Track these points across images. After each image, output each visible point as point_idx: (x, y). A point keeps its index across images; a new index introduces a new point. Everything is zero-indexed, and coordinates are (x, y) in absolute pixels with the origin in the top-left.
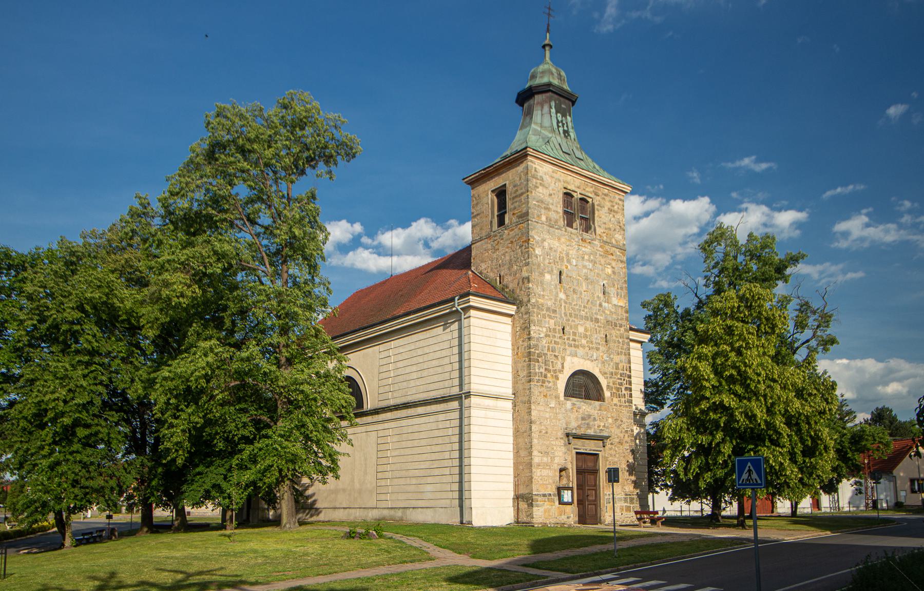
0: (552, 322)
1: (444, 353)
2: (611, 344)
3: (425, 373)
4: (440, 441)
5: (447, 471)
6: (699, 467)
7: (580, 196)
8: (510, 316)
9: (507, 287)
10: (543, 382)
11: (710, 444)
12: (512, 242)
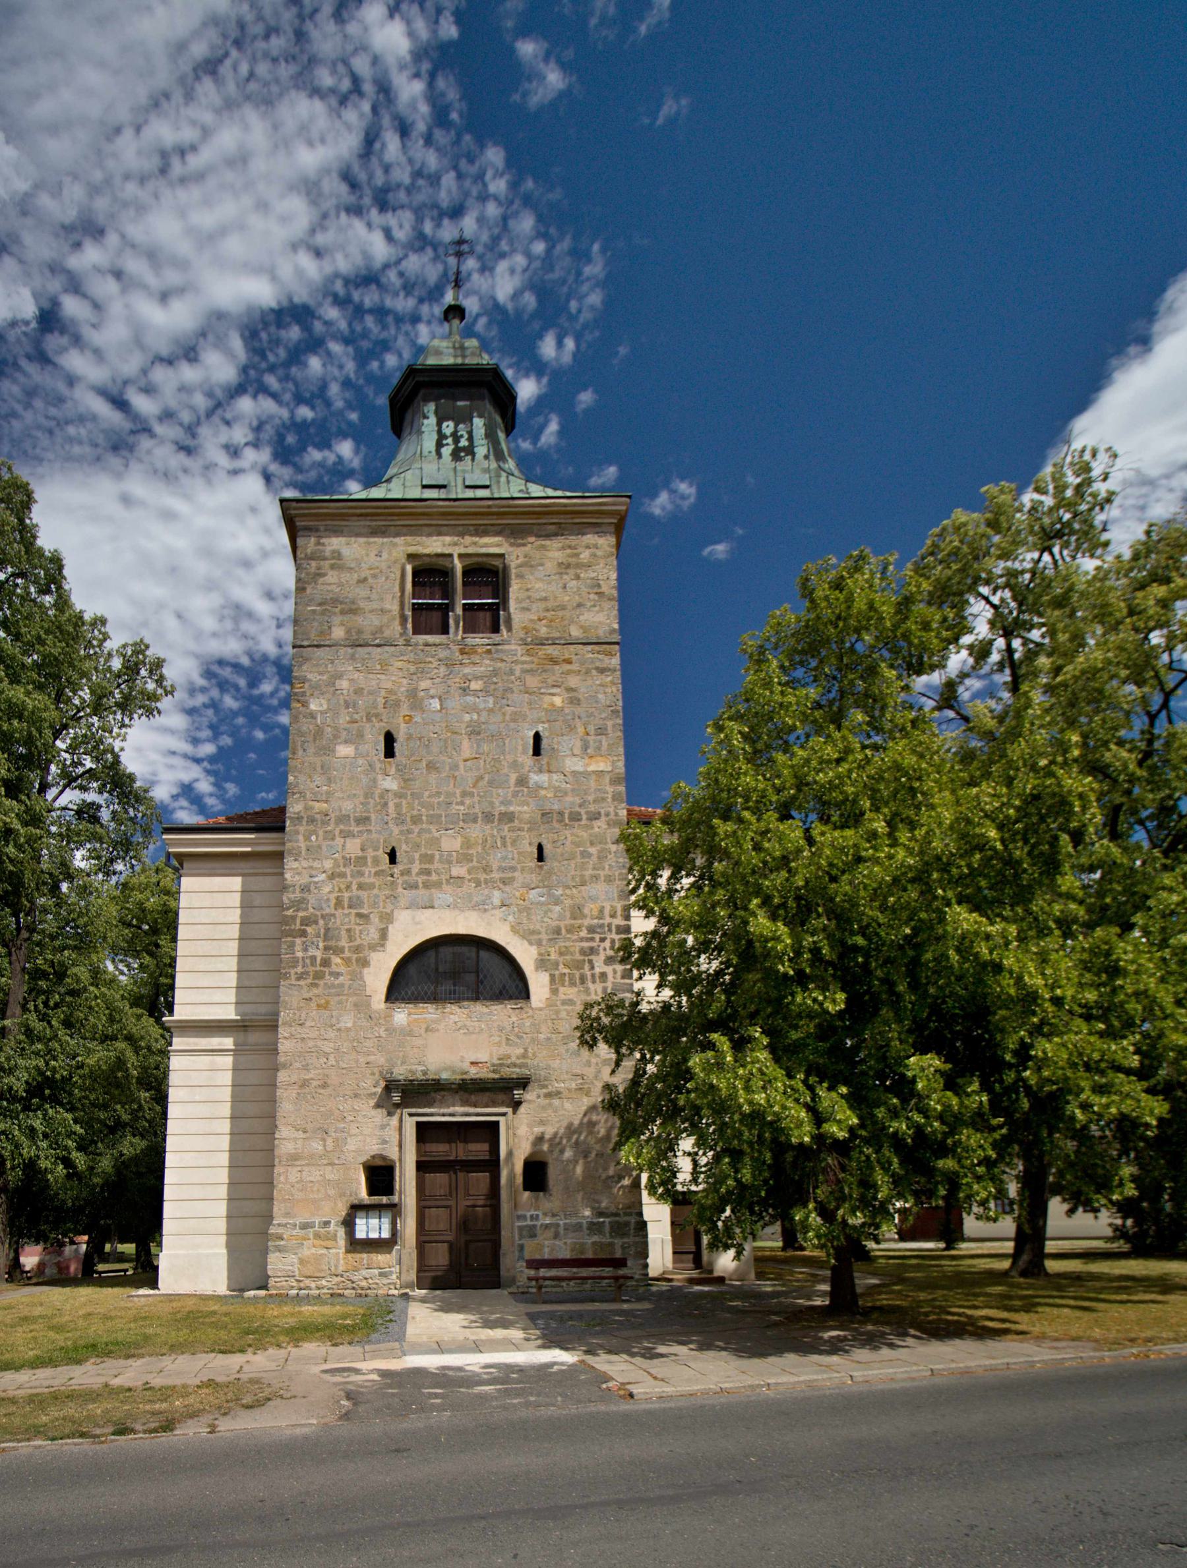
0: (353, 847)
10: (319, 976)
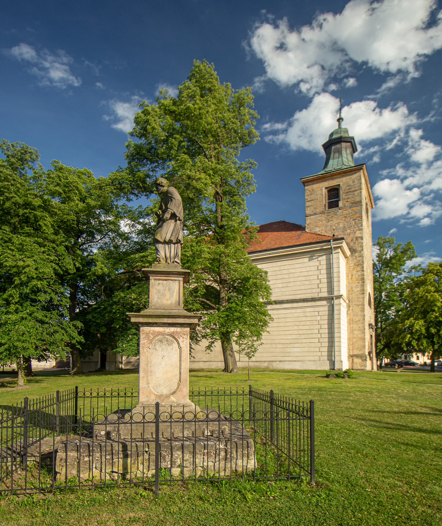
12: (345, 217)
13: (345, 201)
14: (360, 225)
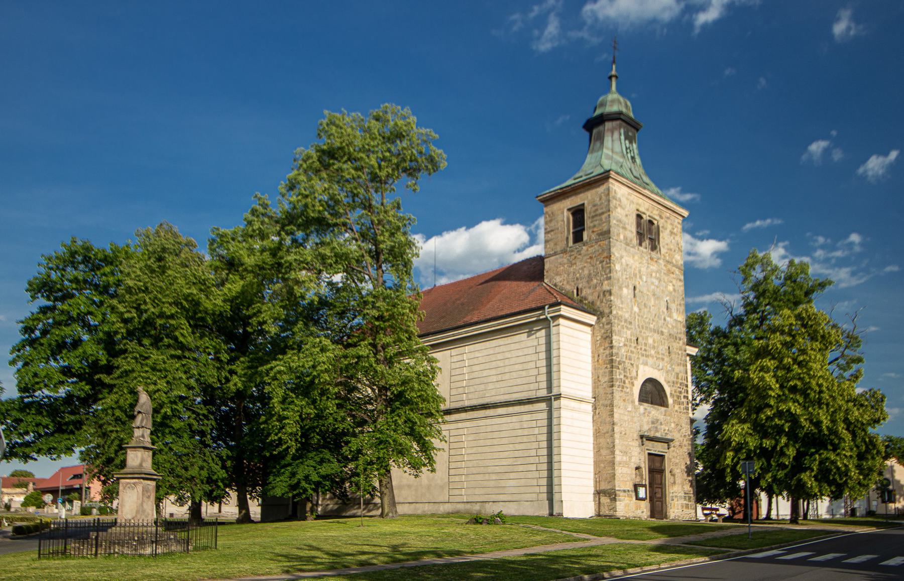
0: (629, 332)
1: (528, 358)
2: (673, 356)
3: (507, 376)
4: (525, 439)
5: (533, 467)
6: (761, 468)
7: (648, 218)
8: (591, 325)
9: (586, 299)
10: (623, 387)
11: (774, 447)
12: (591, 258)
13: (591, 231)
14: (608, 271)
